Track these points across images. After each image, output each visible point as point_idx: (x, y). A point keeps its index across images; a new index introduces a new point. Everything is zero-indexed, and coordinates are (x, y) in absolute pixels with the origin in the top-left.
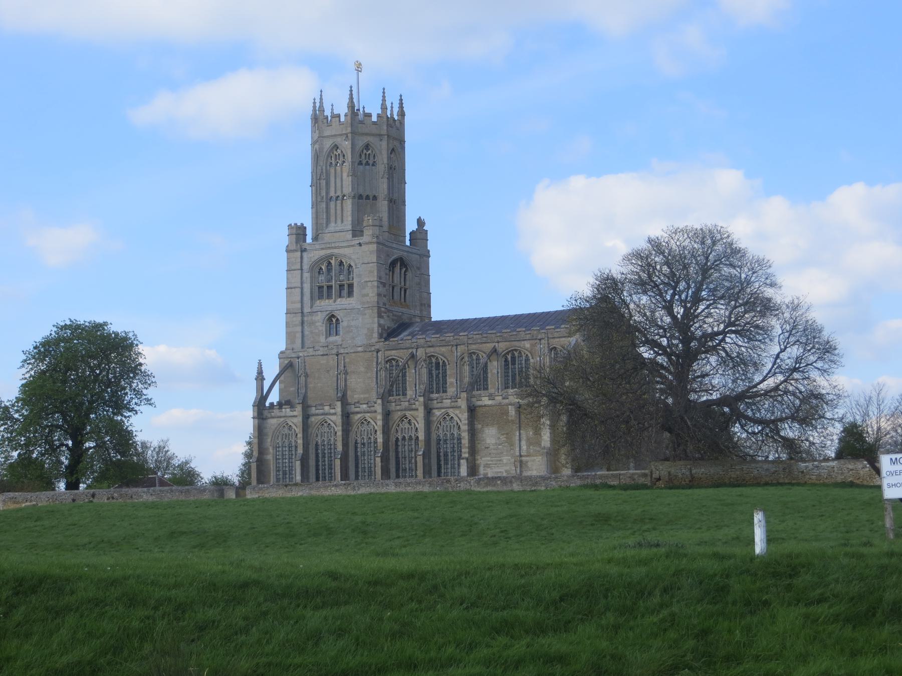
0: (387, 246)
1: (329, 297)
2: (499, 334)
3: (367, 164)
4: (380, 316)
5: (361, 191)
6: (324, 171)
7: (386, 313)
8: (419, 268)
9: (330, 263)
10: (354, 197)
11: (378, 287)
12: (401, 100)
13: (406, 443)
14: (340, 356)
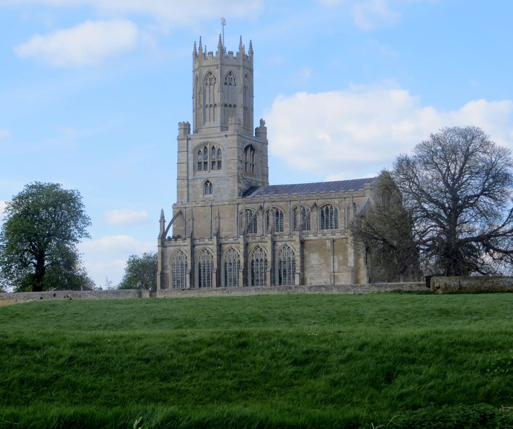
0: (243, 137)
1: (205, 169)
2: (318, 194)
3: (230, 84)
4: (239, 182)
5: (226, 102)
6: (202, 89)
7: (242, 180)
8: (261, 152)
9: (206, 148)
10: (222, 106)
11: (238, 163)
12: (251, 43)
13: (259, 263)
14: (213, 207)
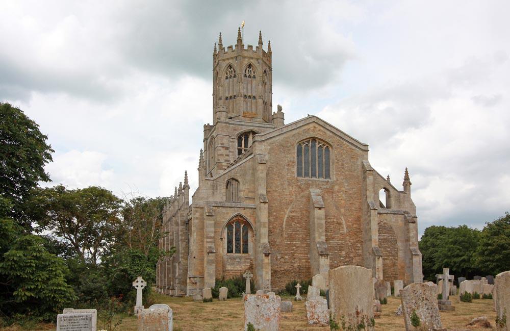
3: (250, 77)
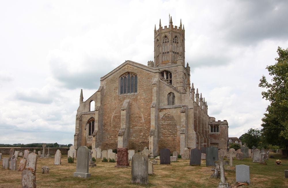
3: (176, 42)
